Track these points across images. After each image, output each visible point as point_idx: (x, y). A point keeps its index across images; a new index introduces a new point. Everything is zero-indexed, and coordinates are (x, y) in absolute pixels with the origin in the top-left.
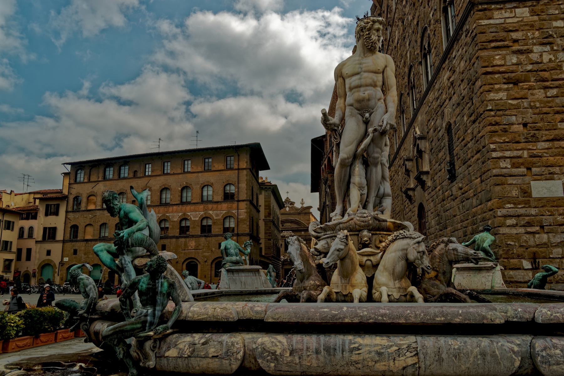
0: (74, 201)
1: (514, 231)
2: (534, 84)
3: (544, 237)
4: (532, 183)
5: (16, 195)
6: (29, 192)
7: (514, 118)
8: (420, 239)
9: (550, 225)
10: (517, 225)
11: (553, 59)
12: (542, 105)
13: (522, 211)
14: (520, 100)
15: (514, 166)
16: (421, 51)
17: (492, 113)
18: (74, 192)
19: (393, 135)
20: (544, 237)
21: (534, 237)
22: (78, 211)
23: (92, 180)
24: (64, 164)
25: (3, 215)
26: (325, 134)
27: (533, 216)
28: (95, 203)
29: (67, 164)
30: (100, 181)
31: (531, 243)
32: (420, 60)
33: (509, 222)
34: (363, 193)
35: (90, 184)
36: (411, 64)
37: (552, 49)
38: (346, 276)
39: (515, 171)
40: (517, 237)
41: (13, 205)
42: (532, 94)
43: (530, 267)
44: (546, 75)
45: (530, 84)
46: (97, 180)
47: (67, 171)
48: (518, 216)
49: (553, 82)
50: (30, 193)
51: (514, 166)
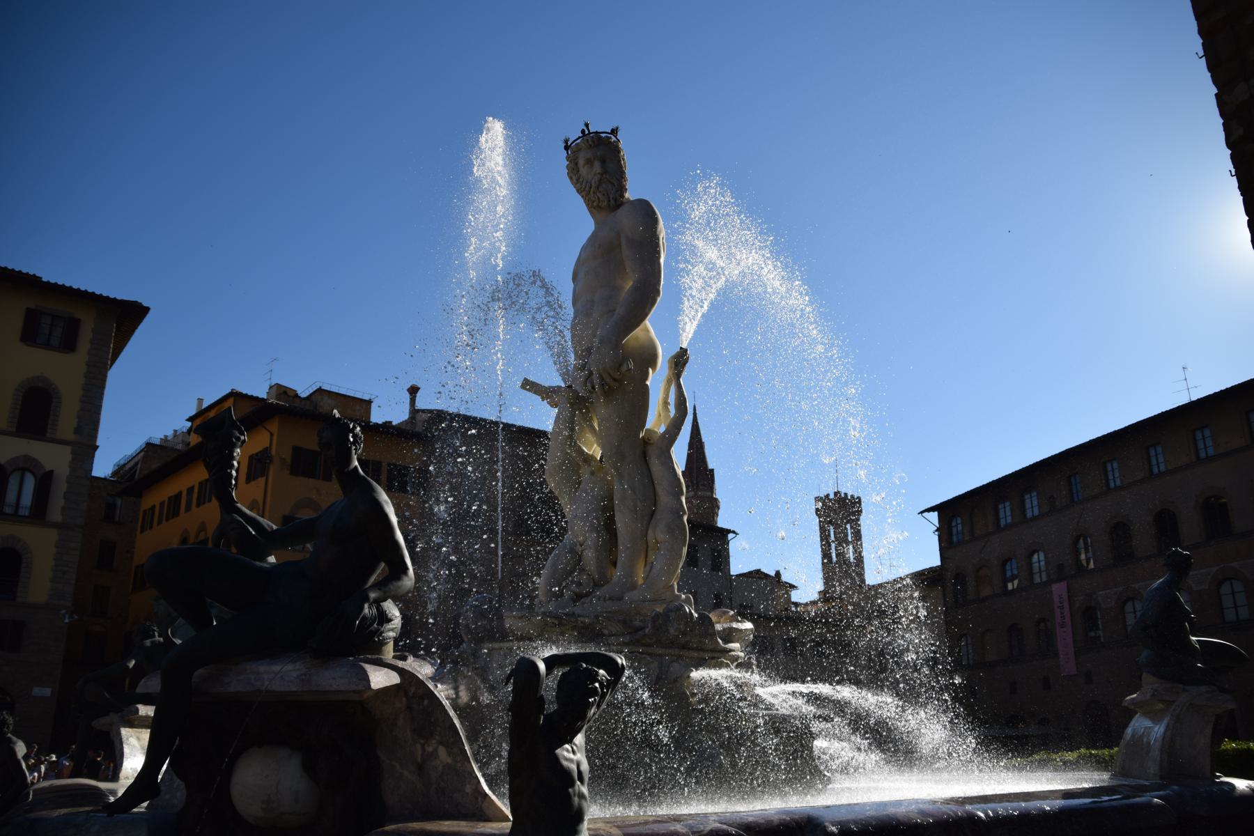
24: (922, 512)
29: (929, 510)
47: (936, 528)
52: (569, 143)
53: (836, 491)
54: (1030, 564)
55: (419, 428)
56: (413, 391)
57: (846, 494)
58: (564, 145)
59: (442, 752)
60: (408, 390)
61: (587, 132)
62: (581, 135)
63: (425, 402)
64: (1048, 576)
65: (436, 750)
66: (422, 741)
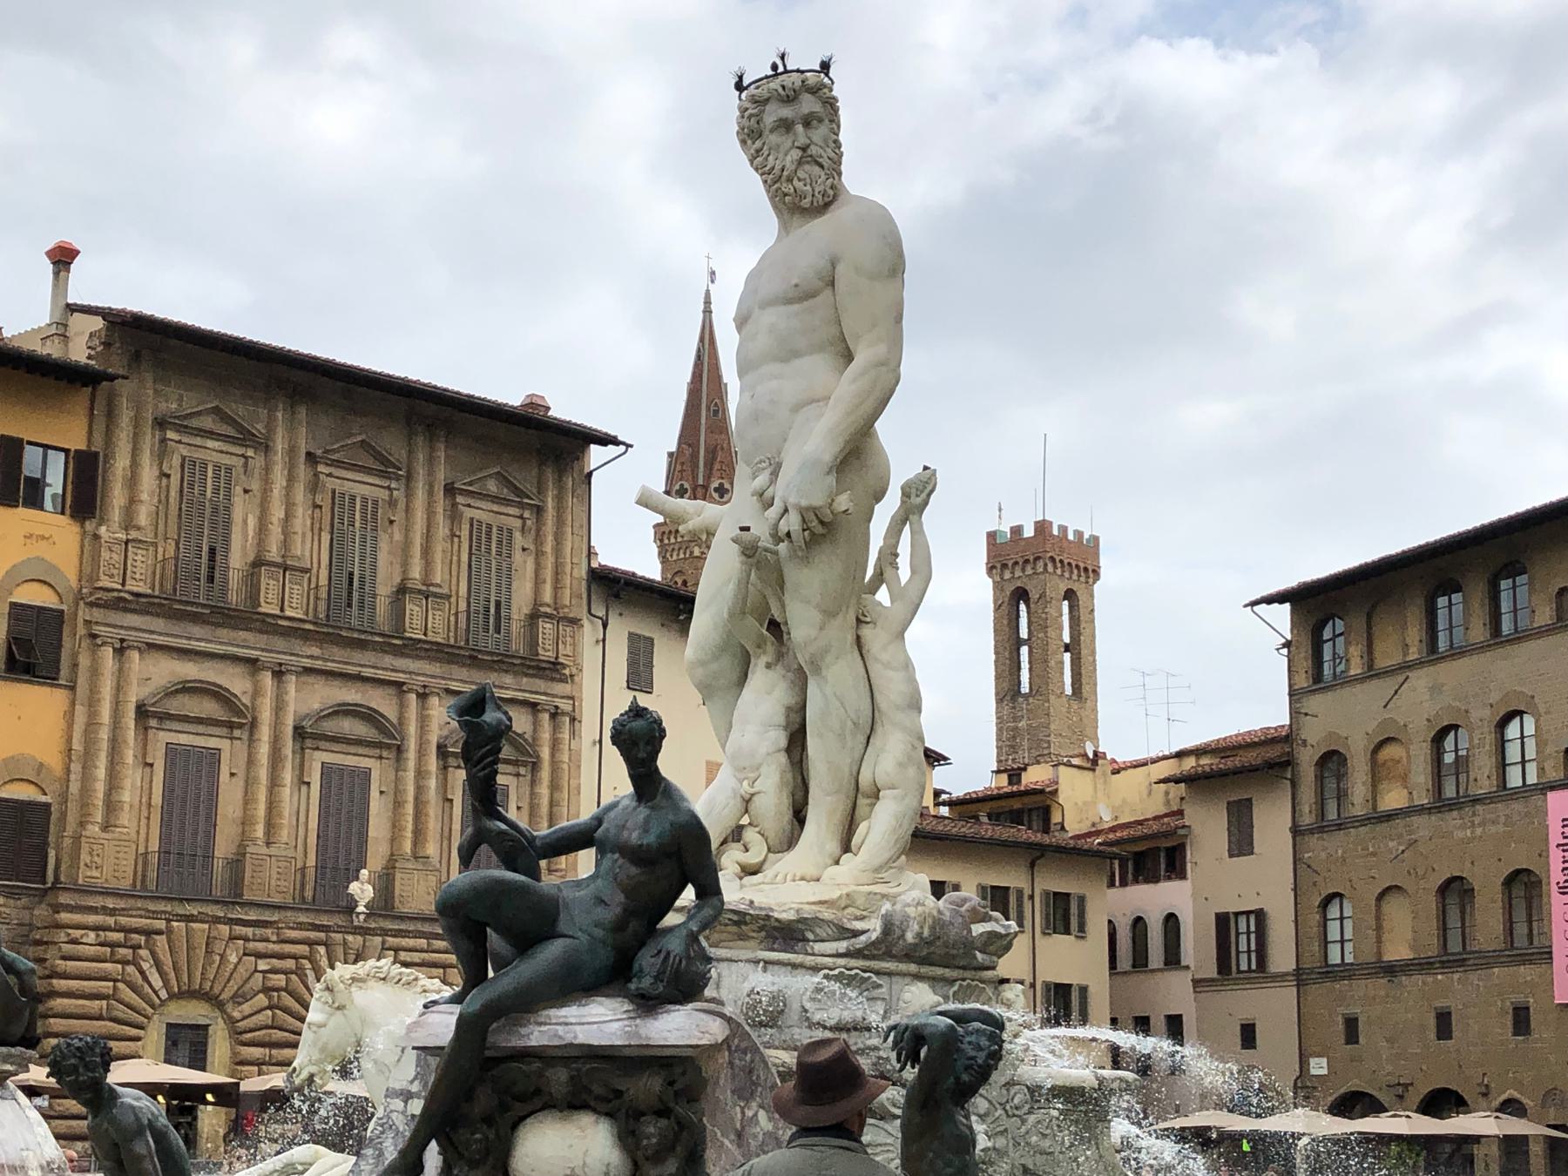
0: (1320, 779)
5: (1116, 772)
6: (1175, 749)
18: (1315, 737)
22: (1340, 827)
23: (1381, 663)
25: (1032, 865)
28: (1404, 779)
29: (1269, 600)
30: (1407, 667)
34: (752, 791)
35: (1375, 682)
41: (1106, 818)
46: (1395, 659)
47: (1283, 641)
50: (1180, 755)
52: (745, 83)
53: (1040, 518)
54: (1502, 743)
55: (78, 353)
56: (63, 258)
57: (1063, 529)
58: (735, 80)
59: (762, 1115)
60: (50, 254)
61: (781, 69)
62: (771, 73)
63: (85, 286)
64: (1541, 770)
65: (756, 1115)
66: (742, 1104)
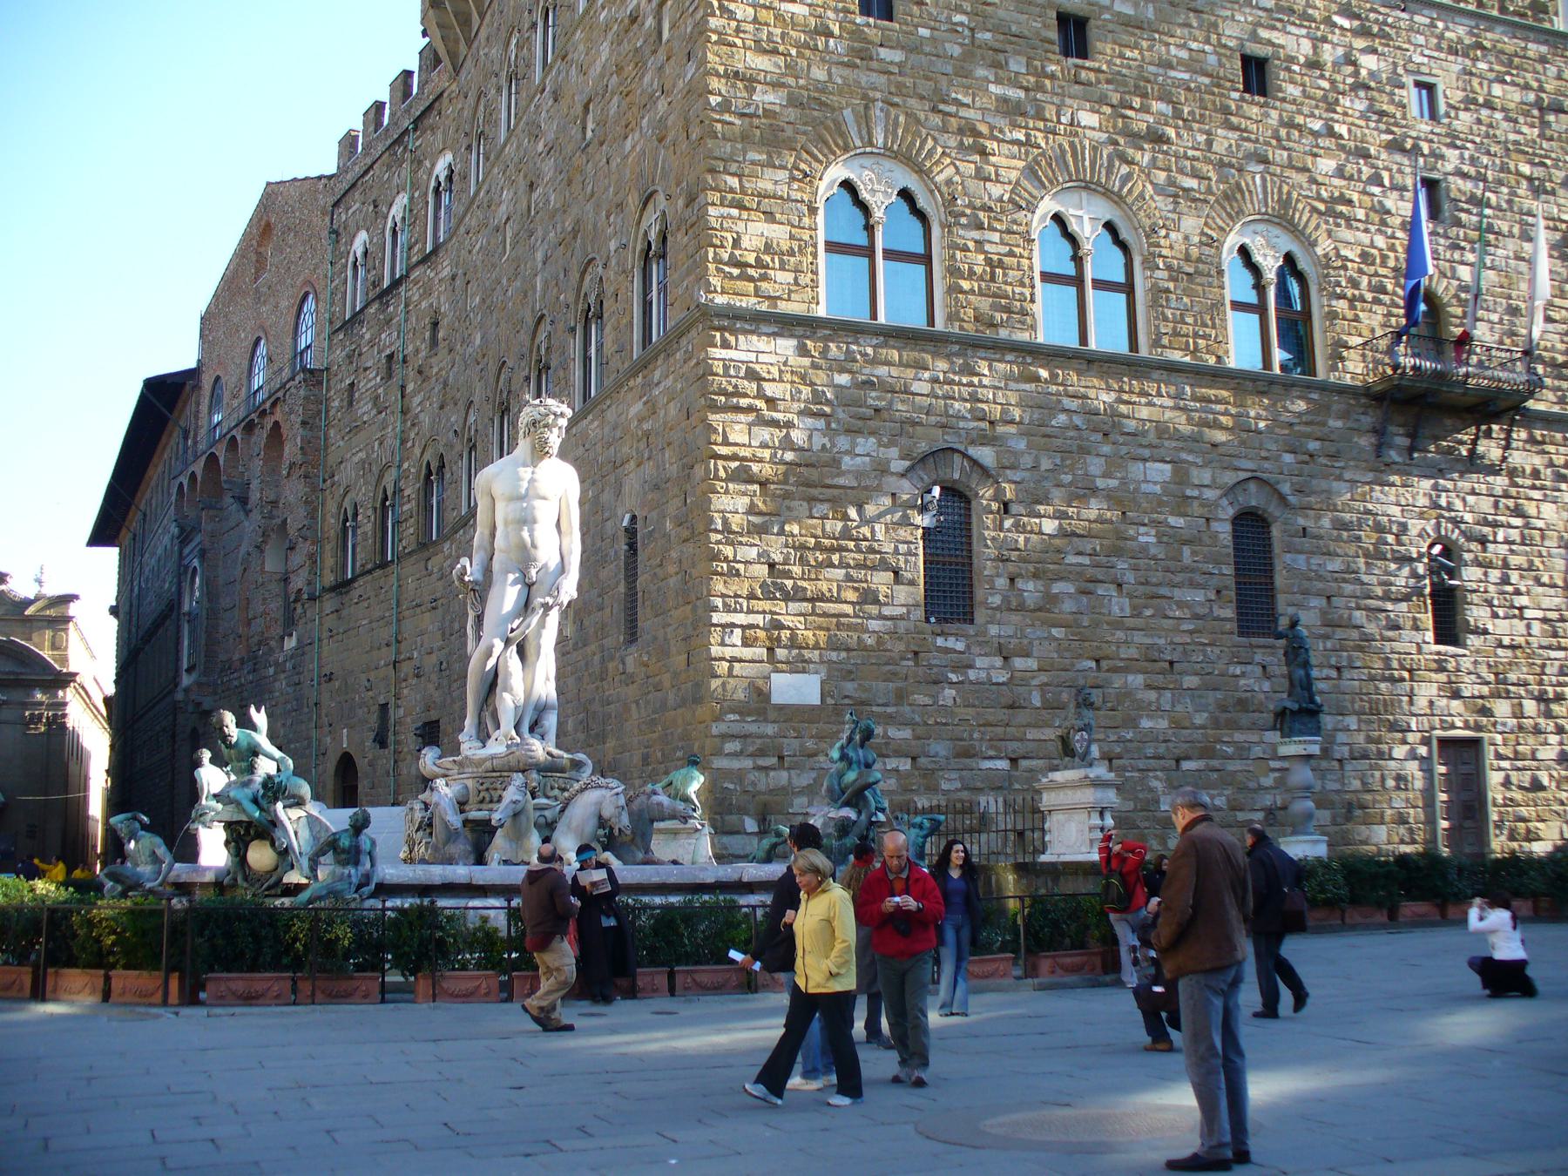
1: (736, 764)
2: (794, 489)
3: (782, 777)
4: (773, 676)
7: (753, 553)
8: (620, 790)
9: (795, 756)
10: (742, 752)
11: (828, 446)
12: (803, 532)
13: (753, 728)
14: (767, 518)
15: (746, 643)
16: (577, 302)
17: (720, 537)
19: (461, 456)
20: (782, 777)
21: (767, 775)
26: (192, 364)
27: (770, 737)
31: (762, 787)
32: (572, 324)
33: (731, 747)
36: (545, 312)
37: (828, 424)
38: (518, 836)
39: (747, 653)
40: (739, 776)
42: (789, 508)
43: (756, 830)
44: (813, 474)
45: (787, 487)
48: (745, 737)
49: (824, 490)
51: (746, 643)
